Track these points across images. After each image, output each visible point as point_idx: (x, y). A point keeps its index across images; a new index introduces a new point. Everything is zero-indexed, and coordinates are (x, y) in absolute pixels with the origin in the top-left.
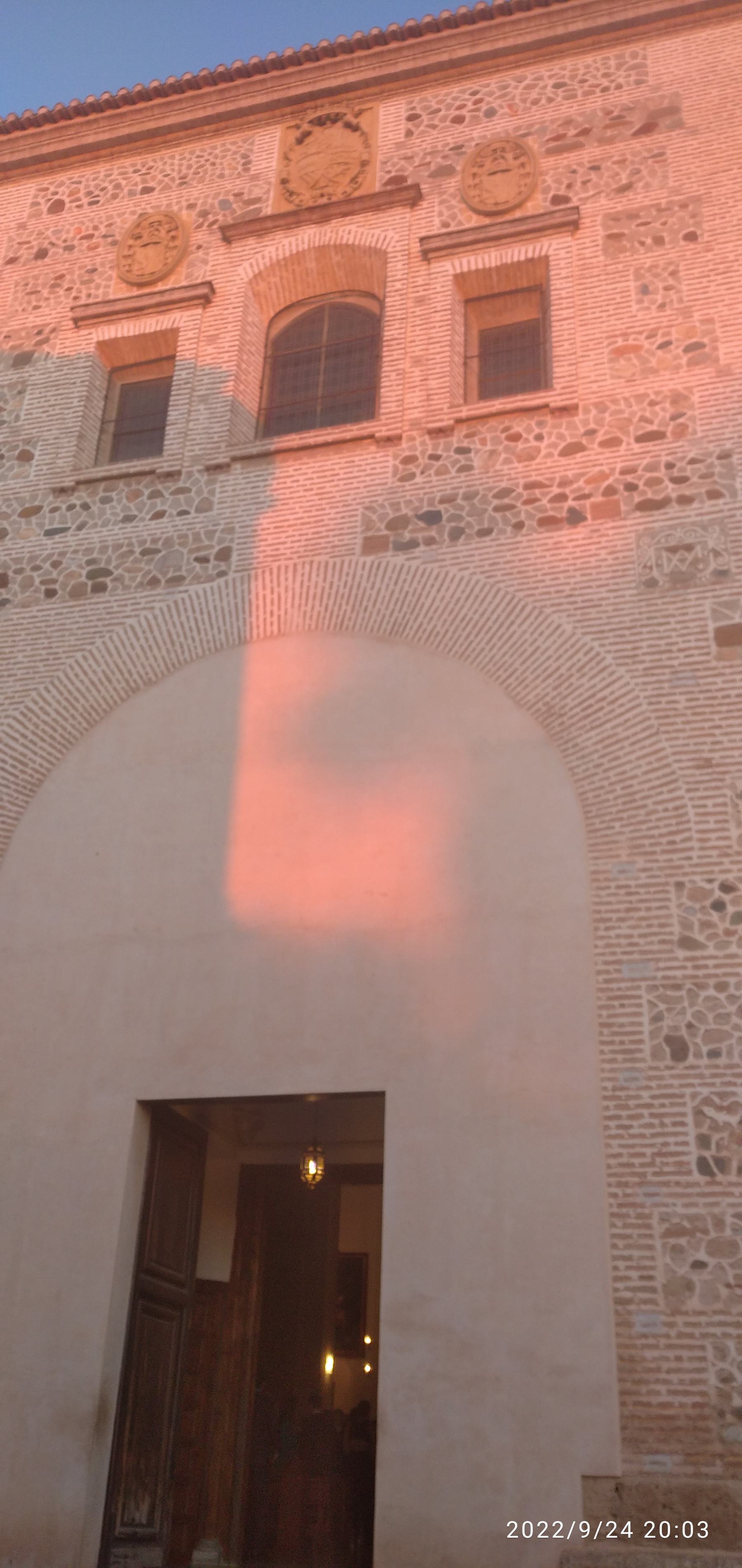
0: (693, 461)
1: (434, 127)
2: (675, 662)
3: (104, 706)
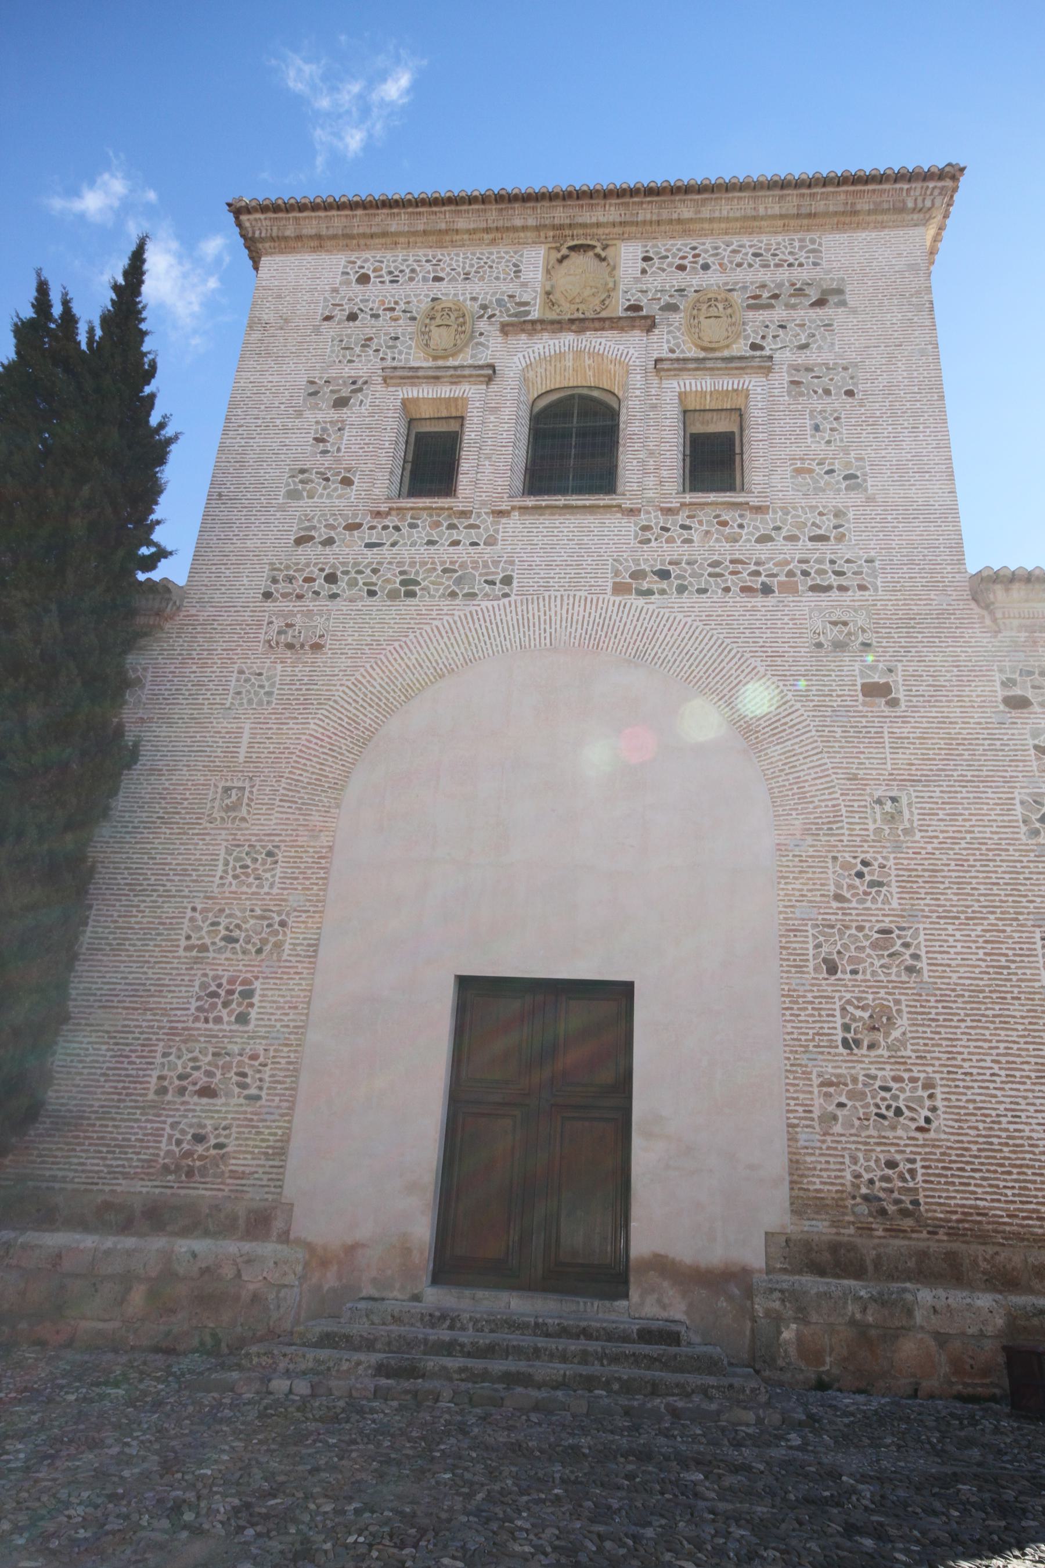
0: (848, 561)
1: (664, 270)
2: (835, 704)
3: (418, 685)
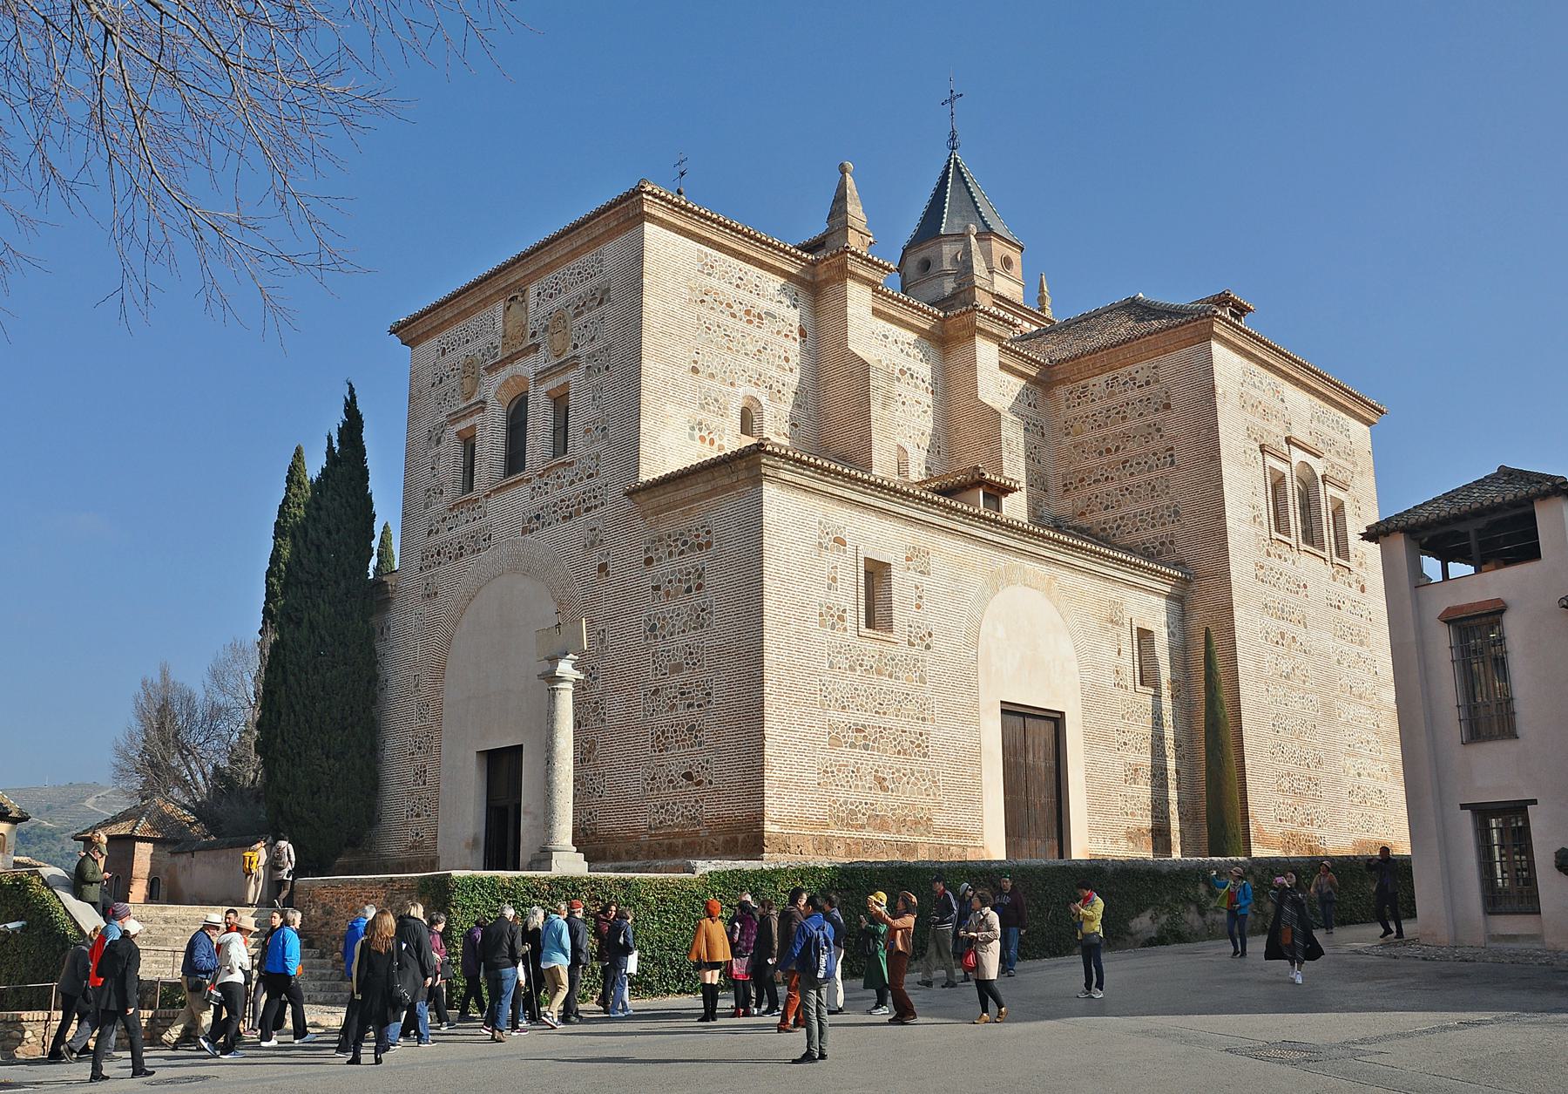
0: (600, 488)
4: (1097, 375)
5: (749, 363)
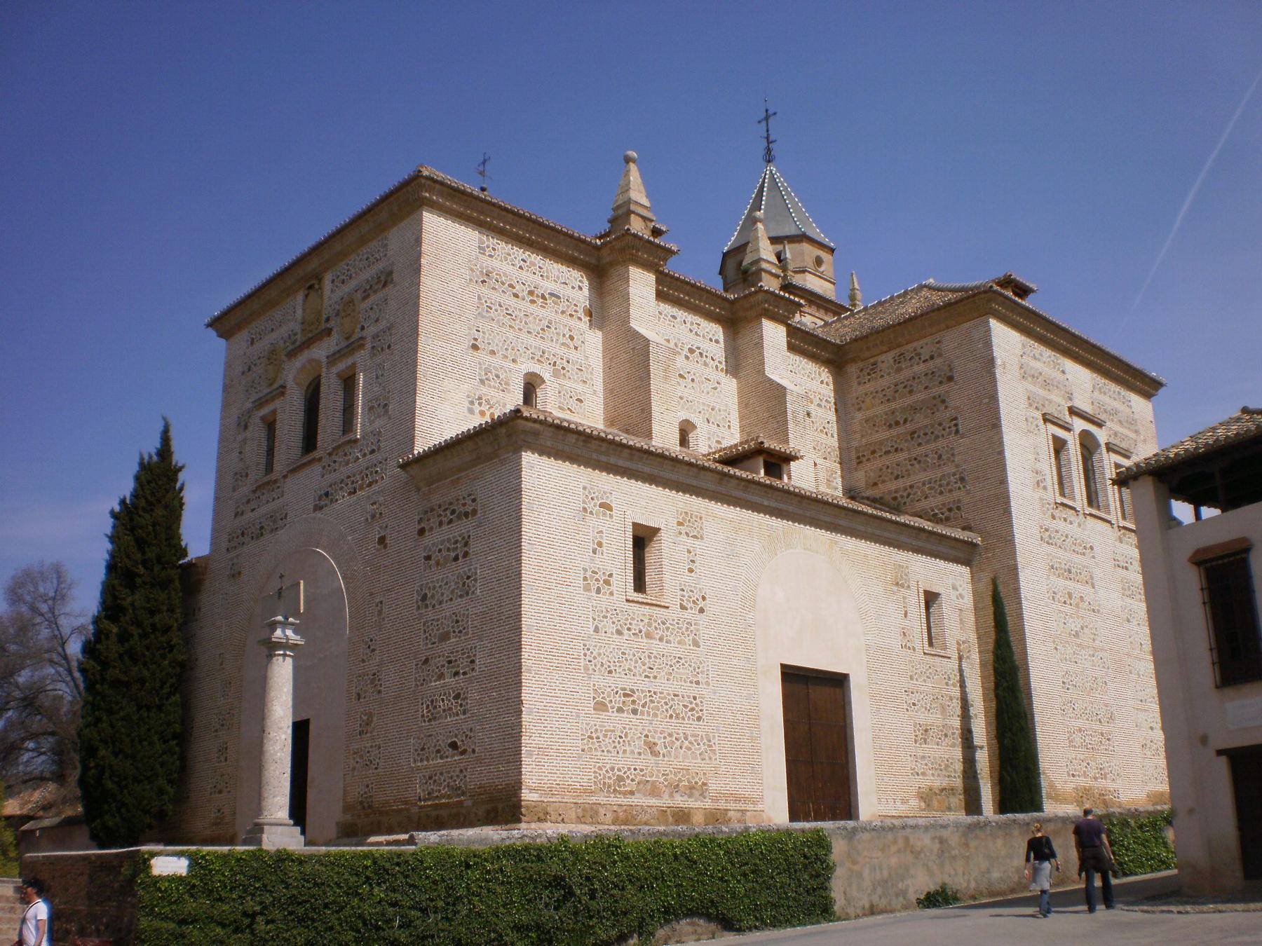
4: (886, 352)
5: (532, 341)
